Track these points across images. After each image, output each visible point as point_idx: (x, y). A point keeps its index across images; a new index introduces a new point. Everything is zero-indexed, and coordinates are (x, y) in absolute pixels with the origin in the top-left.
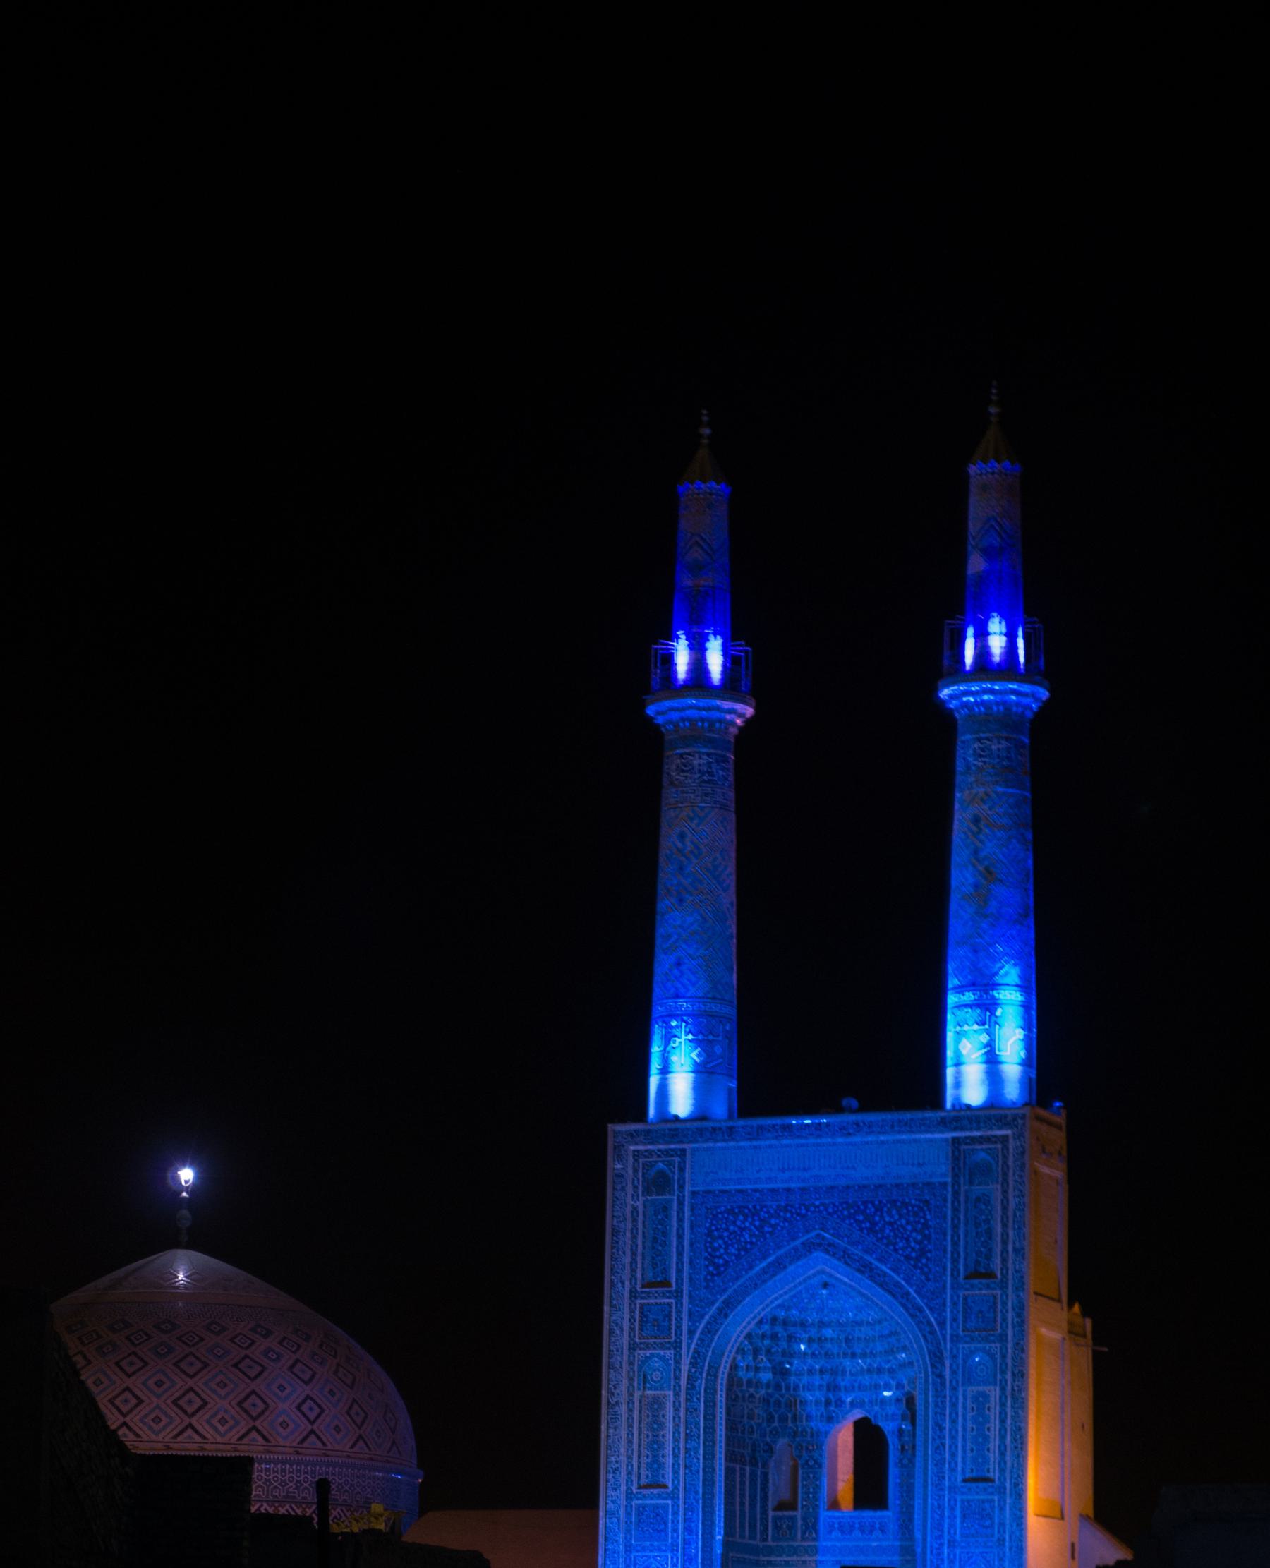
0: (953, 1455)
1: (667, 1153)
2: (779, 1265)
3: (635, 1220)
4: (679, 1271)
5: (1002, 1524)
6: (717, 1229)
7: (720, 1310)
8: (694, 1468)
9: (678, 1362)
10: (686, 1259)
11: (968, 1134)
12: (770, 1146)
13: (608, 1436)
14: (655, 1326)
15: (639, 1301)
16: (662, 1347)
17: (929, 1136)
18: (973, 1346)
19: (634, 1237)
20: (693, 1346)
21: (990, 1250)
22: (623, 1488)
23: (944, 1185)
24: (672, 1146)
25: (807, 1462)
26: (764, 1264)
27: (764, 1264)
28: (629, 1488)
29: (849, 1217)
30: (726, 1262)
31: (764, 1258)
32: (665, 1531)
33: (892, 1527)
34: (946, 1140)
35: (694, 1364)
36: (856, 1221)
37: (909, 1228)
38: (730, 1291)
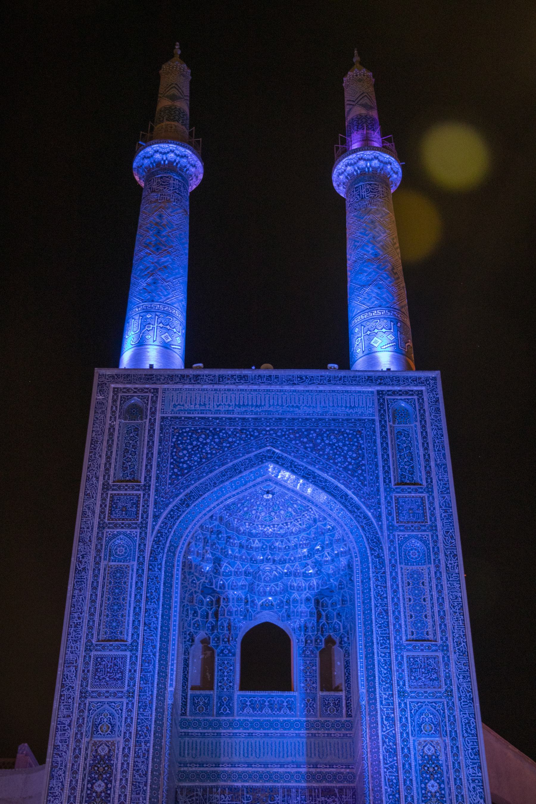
0: (397, 618)
1: (142, 390)
2: (236, 470)
3: (111, 434)
4: (148, 471)
5: (448, 677)
6: (182, 443)
7: (183, 502)
8: (152, 625)
9: (143, 539)
10: (154, 464)
11: (390, 388)
12: (229, 390)
13: (73, 596)
14: (123, 511)
15: (110, 492)
16: (129, 526)
17: (358, 388)
18: (407, 534)
19: (110, 446)
20: (157, 527)
21: (412, 467)
22: (84, 640)
23: (373, 420)
24: (147, 386)
25: (222, 651)
26: (222, 468)
27: (222, 468)
28: (89, 641)
29: (295, 439)
30: (190, 468)
31: (223, 465)
32: (122, 679)
33: (299, 705)
34: (372, 392)
35: (157, 542)
36: (302, 442)
37: (346, 448)
38: (192, 487)
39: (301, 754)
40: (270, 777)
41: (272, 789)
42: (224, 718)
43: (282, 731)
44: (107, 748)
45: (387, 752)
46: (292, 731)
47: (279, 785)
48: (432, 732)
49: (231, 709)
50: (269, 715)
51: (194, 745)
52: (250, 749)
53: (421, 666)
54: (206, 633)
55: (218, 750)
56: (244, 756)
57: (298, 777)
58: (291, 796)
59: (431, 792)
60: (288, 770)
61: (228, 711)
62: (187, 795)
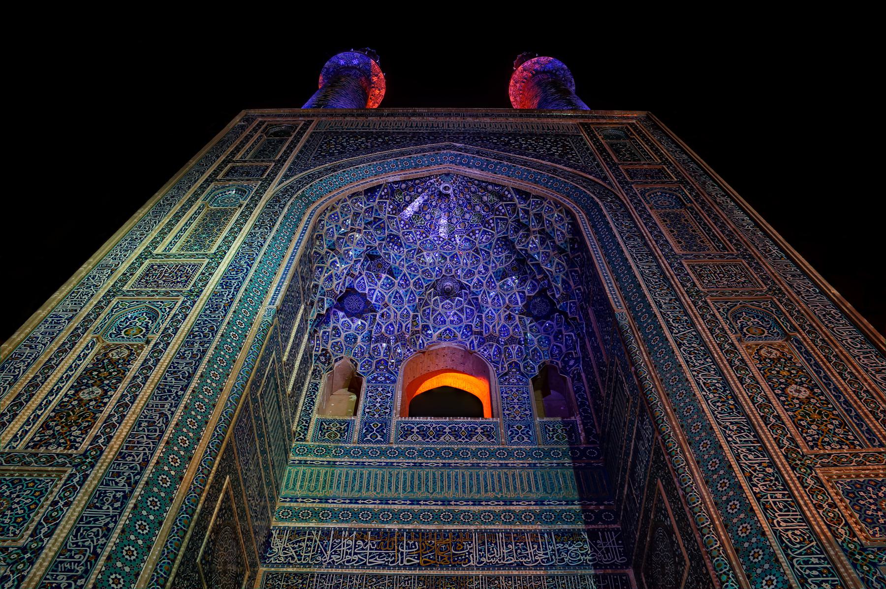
39: (511, 488)
40: (455, 517)
41: (457, 534)
42: (372, 445)
43: (475, 461)
44: (127, 352)
45: (690, 354)
46: (493, 461)
47: (472, 527)
48: (766, 334)
49: (386, 438)
50: (451, 443)
51: (314, 476)
52: (416, 482)
53: (715, 272)
54: (351, 360)
55: (357, 483)
56: (404, 490)
57: (507, 517)
58: (496, 544)
59: (798, 399)
60: (488, 508)
61: (379, 438)
62: (289, 540)
